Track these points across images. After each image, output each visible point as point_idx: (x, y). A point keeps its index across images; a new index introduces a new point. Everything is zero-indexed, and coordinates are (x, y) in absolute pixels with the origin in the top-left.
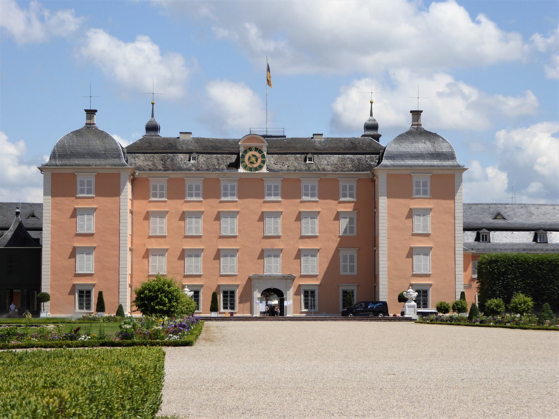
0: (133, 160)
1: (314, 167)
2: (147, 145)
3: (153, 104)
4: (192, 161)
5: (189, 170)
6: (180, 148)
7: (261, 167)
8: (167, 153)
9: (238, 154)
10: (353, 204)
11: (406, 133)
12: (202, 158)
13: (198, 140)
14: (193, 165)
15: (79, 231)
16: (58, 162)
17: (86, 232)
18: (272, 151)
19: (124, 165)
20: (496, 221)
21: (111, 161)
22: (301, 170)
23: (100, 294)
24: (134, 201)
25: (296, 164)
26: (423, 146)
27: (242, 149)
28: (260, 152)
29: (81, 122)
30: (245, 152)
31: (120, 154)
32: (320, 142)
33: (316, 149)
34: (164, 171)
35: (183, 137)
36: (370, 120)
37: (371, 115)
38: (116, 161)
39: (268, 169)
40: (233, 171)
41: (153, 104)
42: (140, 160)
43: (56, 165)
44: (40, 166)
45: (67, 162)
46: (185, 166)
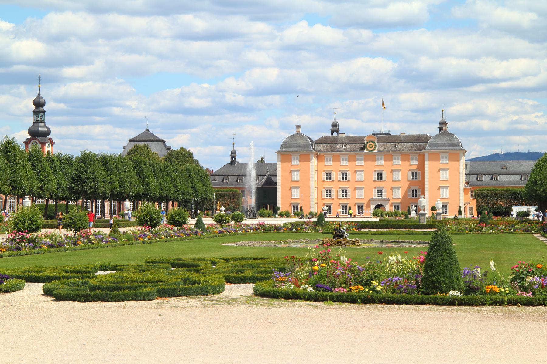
0: (317, 147)
1: (399, 149)
2: (324, 140)
4: (344, 147)
5: (342, 151)
7: (374, 150)
8: (333, 143)
10: (417, 166)
12: (348, 146)
13: (348, 137)
14: (344, 149)
15: (293, 180)
16: (284, 150)
17: (296, 180)
18: (380, 141)
19: (312, 151)
20: (502, 170)
21: (306, 149)
23: (301, 207)
25: (391, 148)
26: (445, 140)
27: (366, 142)
28: (374, 143)
29: (294, 131)
30: (367, 143)
31: (310, 146)
32: (403, 137)
33: (400, 141)
38: (308, 149)
39: (378, 151)
40: (361, 152)
41: (335, 113)
42: (321, 147)
43: (283, 151)
44: (276, 151)
46: (340, 150)
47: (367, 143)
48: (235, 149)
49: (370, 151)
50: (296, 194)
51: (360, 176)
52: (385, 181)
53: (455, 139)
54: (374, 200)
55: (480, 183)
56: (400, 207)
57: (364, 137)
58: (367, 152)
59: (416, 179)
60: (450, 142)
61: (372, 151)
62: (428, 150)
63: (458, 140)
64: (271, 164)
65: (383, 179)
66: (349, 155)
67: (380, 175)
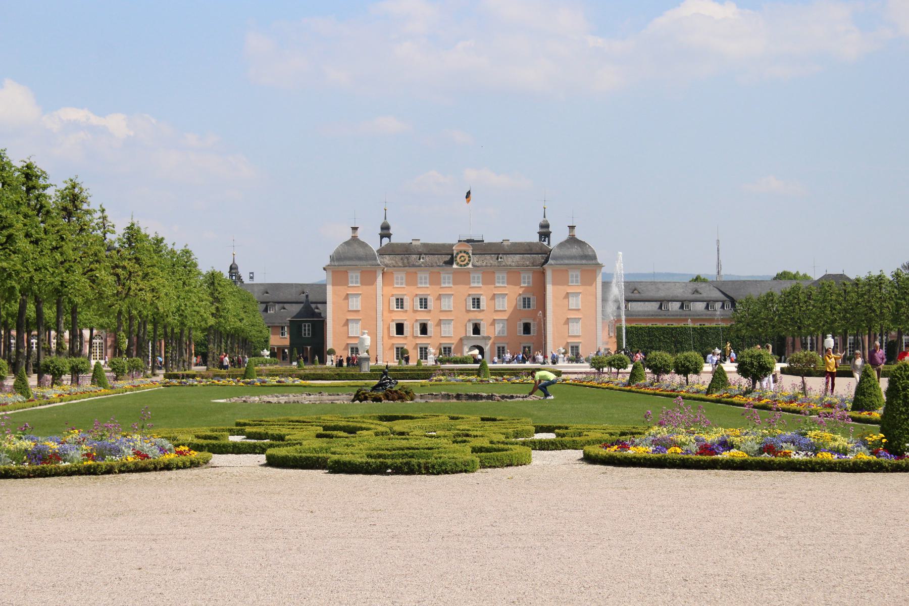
1: (504, 264)
3: (385, 210)
4: (421, 260)
5: (420, 266)
6: (413, 250)
7: (468, 264)
8: (405, 254)
9: (452, 255)
11: (565, 241)
14: (423, 263)
15: (350, 309)
16: (336, 263)
17: (355, 309)
18: (475, 252)
19: (379, 265)
20: (633, 295)
21: (370, 262)
22: (495, 266)
24: (384, 288)
25: (491, 262)
26: (575, 250)
27: (455, 252)
28: (468, 254)
29: (348, 236)
30: (457, 254)
32: (508, 245)
34: (404, 267)
35: (414, 243)
36: (544, 221)
37: (545, 217)
40: (448, 268)
41: (385, 210)
45: (342, 263)
47: (457, 254)
48: (236, 262)
49: (461, 265)
50: (576, 329)
51: (447, 304)
52: (483, 310)
53: (589, 250)
54: (468, 338)
55: (687, 313)
56: (532, 348)
57: (453, 245)
58: (457, 267)
59: (529, 307)
60: (581, 253)
61: (465, 265)
62: (552, 265)
63: (594, 251)
64: (292, 285)
65: (481, 308)
66: (484, 272)
67: (477, 302)
